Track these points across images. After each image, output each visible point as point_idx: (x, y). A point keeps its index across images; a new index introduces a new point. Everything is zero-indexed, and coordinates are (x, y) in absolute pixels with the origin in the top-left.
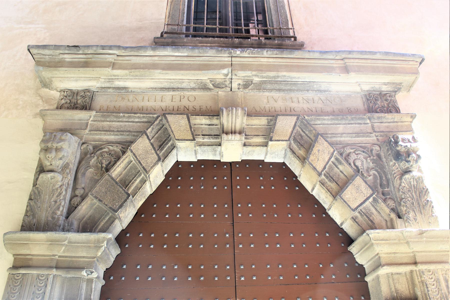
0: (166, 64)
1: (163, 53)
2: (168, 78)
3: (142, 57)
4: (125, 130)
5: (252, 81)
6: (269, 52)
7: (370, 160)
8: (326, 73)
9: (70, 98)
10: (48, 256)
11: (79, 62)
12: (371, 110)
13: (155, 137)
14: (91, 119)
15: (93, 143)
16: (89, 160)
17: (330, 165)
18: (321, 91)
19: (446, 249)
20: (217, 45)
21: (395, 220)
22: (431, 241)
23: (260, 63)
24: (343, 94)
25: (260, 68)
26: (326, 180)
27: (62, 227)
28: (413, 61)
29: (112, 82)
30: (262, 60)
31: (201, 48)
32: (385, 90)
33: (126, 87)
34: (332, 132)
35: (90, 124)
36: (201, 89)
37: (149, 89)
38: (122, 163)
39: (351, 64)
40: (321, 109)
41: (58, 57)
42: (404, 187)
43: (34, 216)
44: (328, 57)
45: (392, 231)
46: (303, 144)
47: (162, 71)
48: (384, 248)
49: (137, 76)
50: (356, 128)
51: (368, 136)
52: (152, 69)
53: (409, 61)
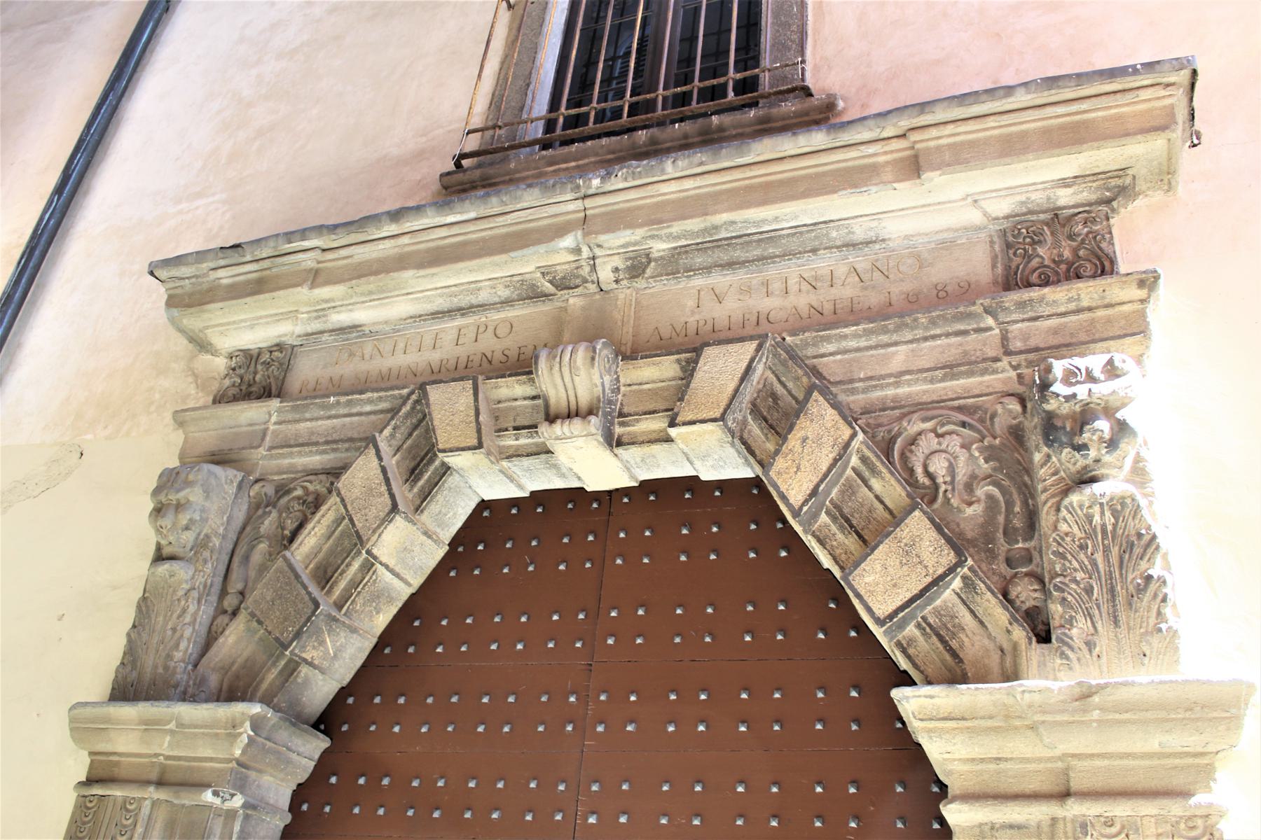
0: (428, 251)
1: (421, 222)
2: (443, 285)
3: (375, 243)
4: (342, 436)
5: (648, 255)
6: (680, 163)
7: (979, 452)
8: (849, 191)
9: (242, 371)
10: (145, 758)
11: (248, 282)
12: (1011, 281)
13: (405, 446)
14: (274, 419)
15: (276, 478)
16: (260, 521)
17: (847, 479)
18: (854, 245)
19: (1183, 747)
20: (593, 159)
21: (1024, 647)
22: (1119, 722)
23: (660, 198)
24: (929, 242)
25: (656, 217)
26: (834, 528)
27: (181, 688)
28: (1158, 84)
29: (324, 316)
30: (664, 188)
31: (503, 191)
32: (1071, 204)
33: (357, 323)
34: (870, 374)
35: (274, 432)
36: (525, 299)
37: (405, 320)
38: (320, 526)
39: (932, 144)
40: (852, 302)
41: (208, 279)
42: (1067, 534)
43: (134, 663)
44: (856, 137)
45: (977, 689)
46: (774, 424)
47: (415, 271)
48: (955, 744)
49: (371, 293)
50: (945, 348)
51: (986, 369)
52: (394, 271)
53: (1138, 88)
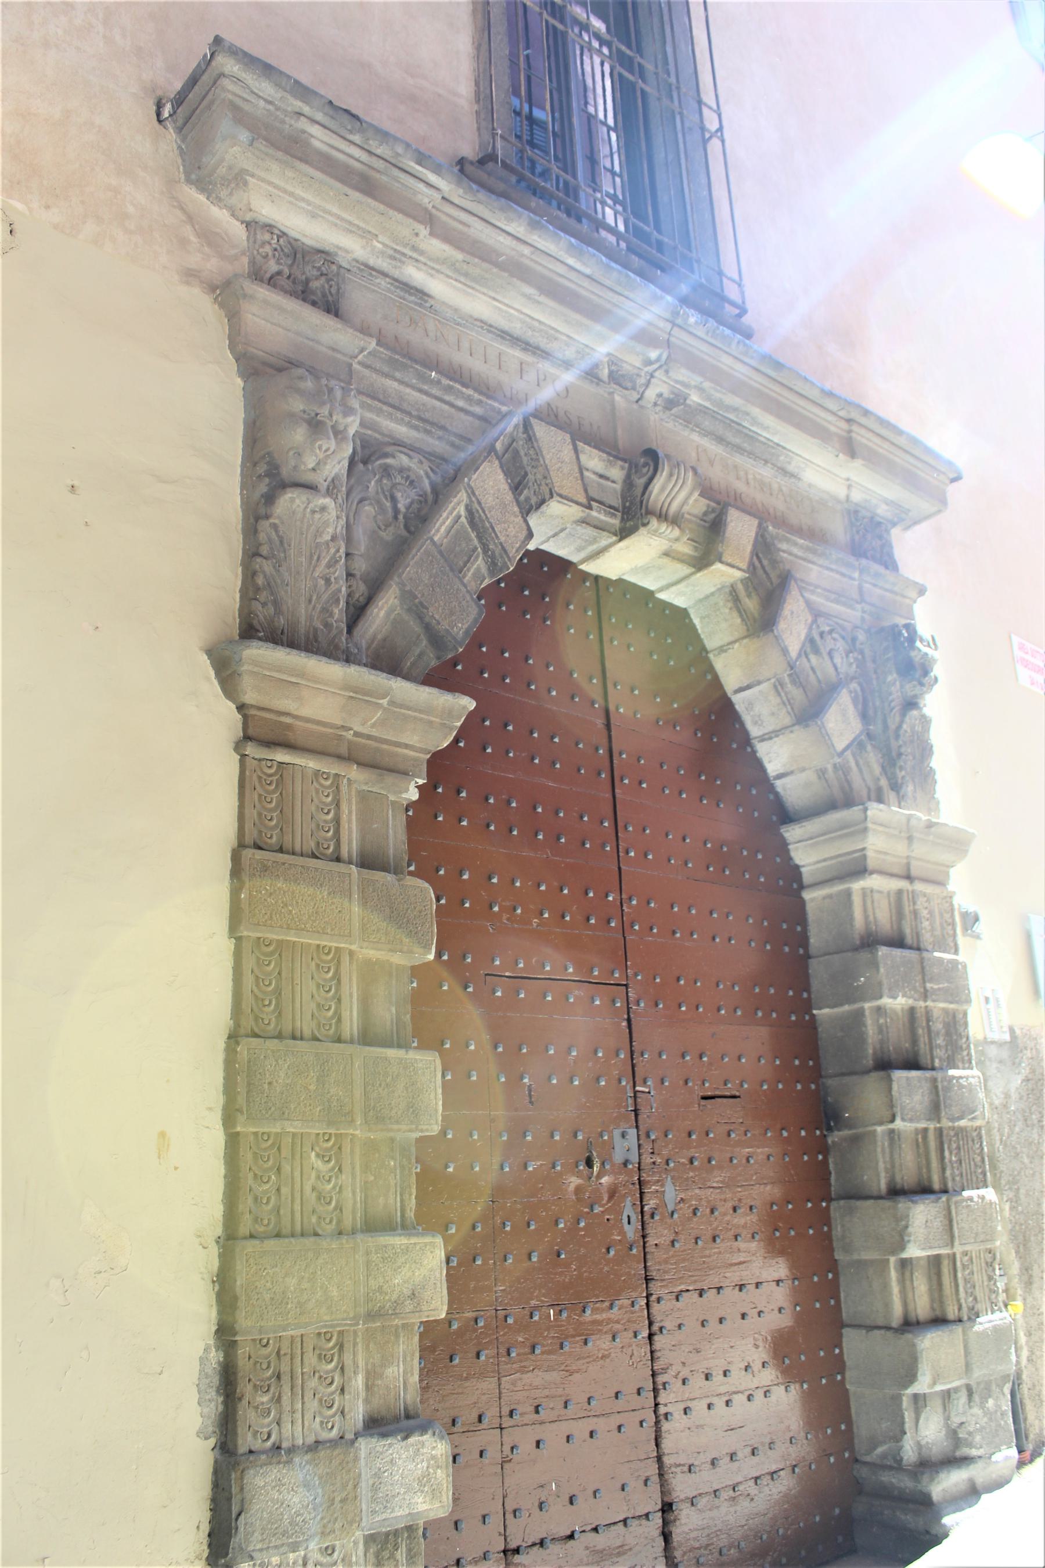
3: (498, 231)
29: (400, 261)
33: (426, 290)
